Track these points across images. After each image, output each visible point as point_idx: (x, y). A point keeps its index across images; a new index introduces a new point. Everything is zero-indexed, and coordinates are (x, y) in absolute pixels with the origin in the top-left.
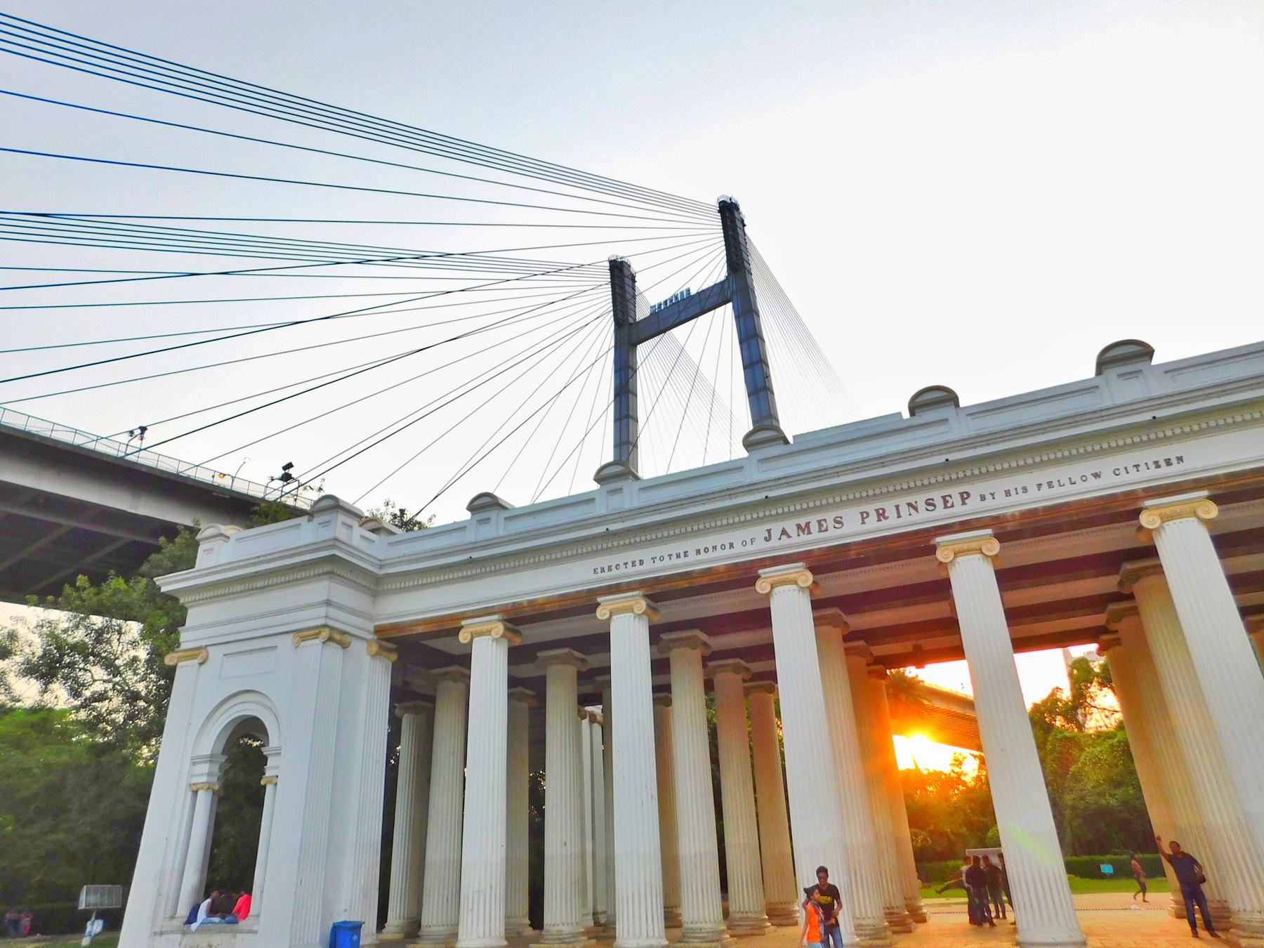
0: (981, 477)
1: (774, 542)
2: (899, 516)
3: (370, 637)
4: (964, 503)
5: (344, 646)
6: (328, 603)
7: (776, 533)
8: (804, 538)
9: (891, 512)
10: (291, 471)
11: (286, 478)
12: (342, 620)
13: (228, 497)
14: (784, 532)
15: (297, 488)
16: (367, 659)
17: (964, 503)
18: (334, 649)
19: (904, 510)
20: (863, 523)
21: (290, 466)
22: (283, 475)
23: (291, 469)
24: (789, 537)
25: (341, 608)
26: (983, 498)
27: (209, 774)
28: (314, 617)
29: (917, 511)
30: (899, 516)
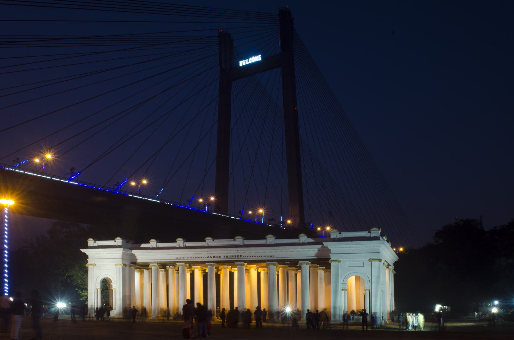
1: (209, 258)
2: (230, 257)
4: (241, 257)
7: (209, 257)
8: (214, 258)
9: (229, 257)
14: (211, 257)
17: (241, 257)
19: (231, 256)
20: (224, 257)
24: (211, 258)
26: (244, 257)
29: (233, 257)
30: (230, 257)
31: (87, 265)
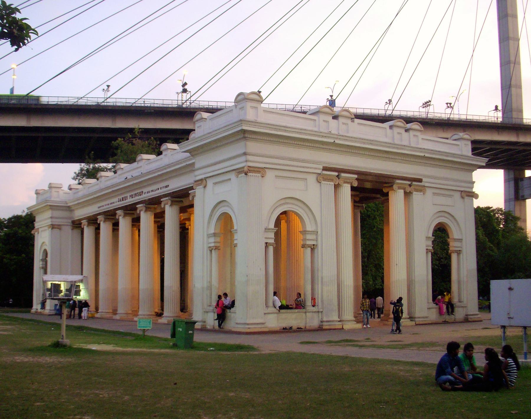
0: (144, 187)
3: (69, 224)
5: (60, 229)
6: (51, 218)
10: (186, 87)
11: (185, 91)
12: (57, 222)
13: (153, 111)
15: (191, 97)
16: (70, 231)
18: (56, 231)
21: (185, 84)
22: (183, 90)
23: (186, 86)
25: (56, 218)
27: (42, 264)
28: (49, 222)
31: (33, 232)
